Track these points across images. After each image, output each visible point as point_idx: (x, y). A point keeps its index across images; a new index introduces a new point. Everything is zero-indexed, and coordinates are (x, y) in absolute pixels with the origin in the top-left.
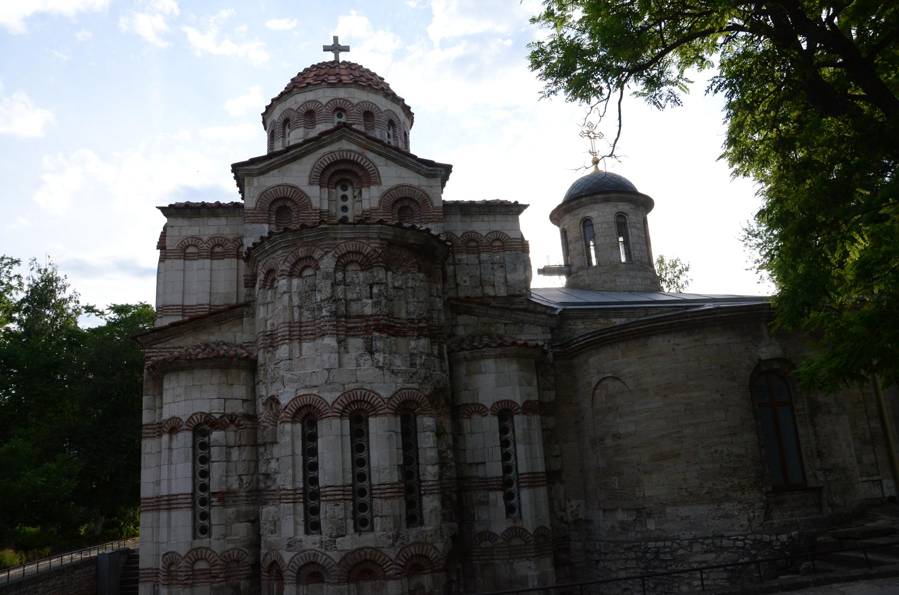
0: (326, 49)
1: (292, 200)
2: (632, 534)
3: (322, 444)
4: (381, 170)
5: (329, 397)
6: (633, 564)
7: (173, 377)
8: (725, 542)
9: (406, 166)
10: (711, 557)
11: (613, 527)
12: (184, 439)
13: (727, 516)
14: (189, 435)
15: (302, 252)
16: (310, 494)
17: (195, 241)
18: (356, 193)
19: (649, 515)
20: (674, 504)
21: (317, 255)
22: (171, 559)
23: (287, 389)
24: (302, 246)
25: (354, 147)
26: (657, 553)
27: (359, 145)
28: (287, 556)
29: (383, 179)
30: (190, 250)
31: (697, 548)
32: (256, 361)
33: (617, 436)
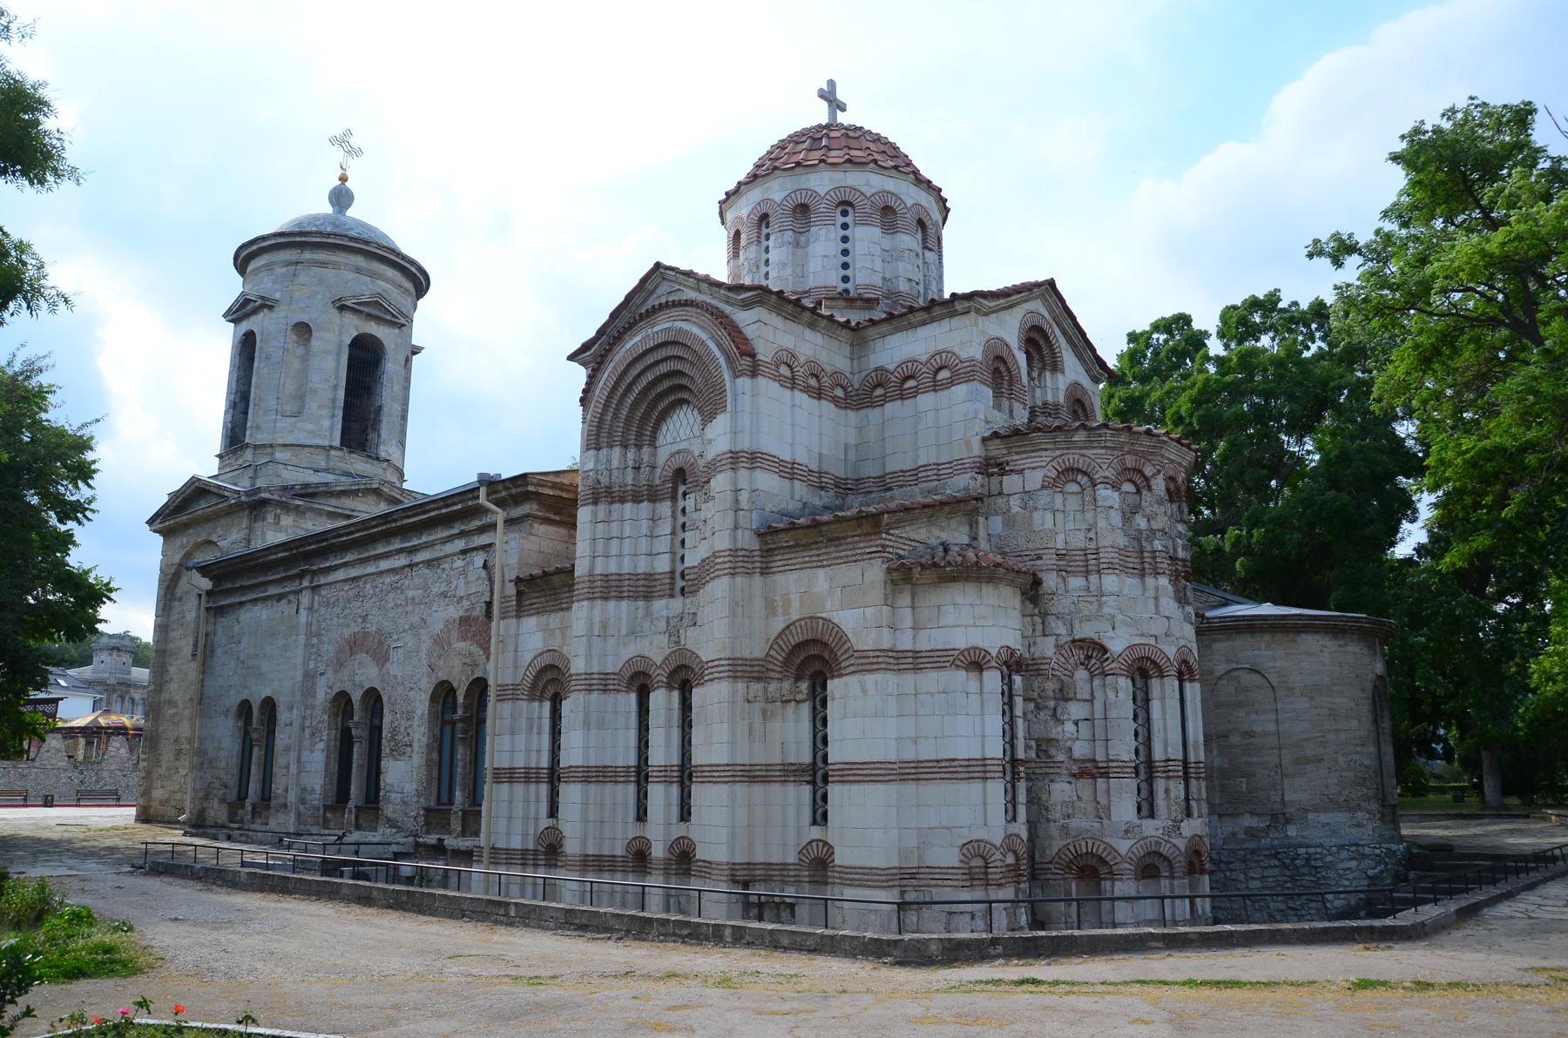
0: (822, 95)
1: (1005, 362)
2: (1265, 842)
3: (1155, 706)
4: (1065, 354)
5: (1171, 651)
6: (1276, 872)
7: (970, 588)
8: (1367, 850)
9: (1080, 357)
10: (1354, 864)
11: (1234, 834)
12: (993, 679)
13: (1359, 825)
14: (999, 674)
15: (1130, 461)
16: (1146, 769)
17: (788, 359)
18: (1035, 374)
19: (1288, 821)
20: (1316, 810)
21: (1148, 470)
22: (975, 851)
23: (1119, 631)
24: (1129, 453)
25: (1047, 315)
26: (1308, 860)
27: (1051, 311)
28: (1124, 846)
29: (1066, 369)
30: (784, 370)
31: (1344, 854)
32: (1037, 582)
33: (1249, 734)
